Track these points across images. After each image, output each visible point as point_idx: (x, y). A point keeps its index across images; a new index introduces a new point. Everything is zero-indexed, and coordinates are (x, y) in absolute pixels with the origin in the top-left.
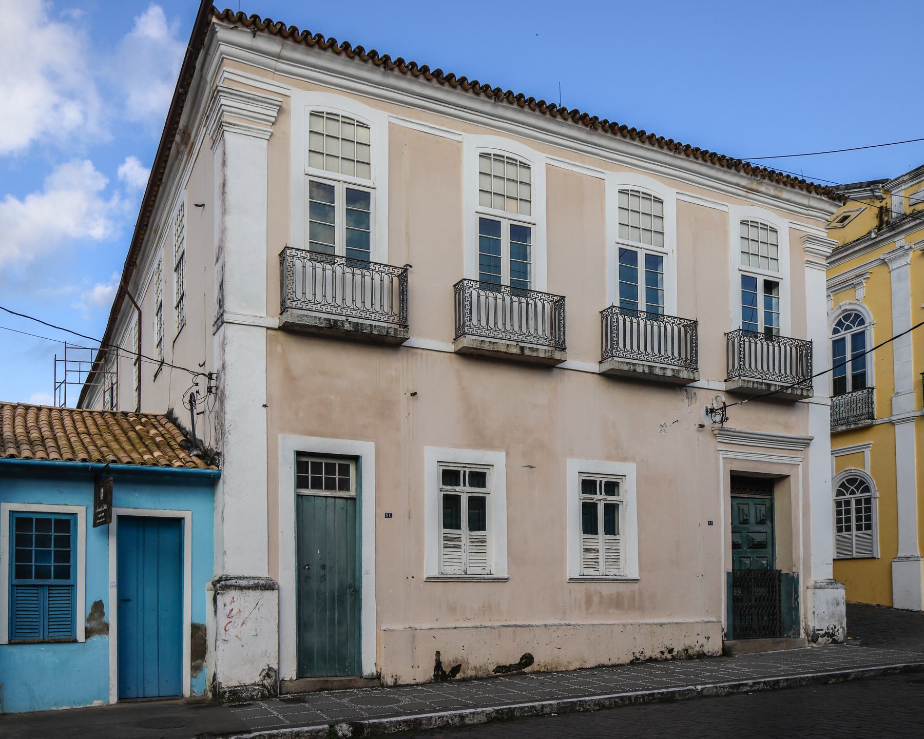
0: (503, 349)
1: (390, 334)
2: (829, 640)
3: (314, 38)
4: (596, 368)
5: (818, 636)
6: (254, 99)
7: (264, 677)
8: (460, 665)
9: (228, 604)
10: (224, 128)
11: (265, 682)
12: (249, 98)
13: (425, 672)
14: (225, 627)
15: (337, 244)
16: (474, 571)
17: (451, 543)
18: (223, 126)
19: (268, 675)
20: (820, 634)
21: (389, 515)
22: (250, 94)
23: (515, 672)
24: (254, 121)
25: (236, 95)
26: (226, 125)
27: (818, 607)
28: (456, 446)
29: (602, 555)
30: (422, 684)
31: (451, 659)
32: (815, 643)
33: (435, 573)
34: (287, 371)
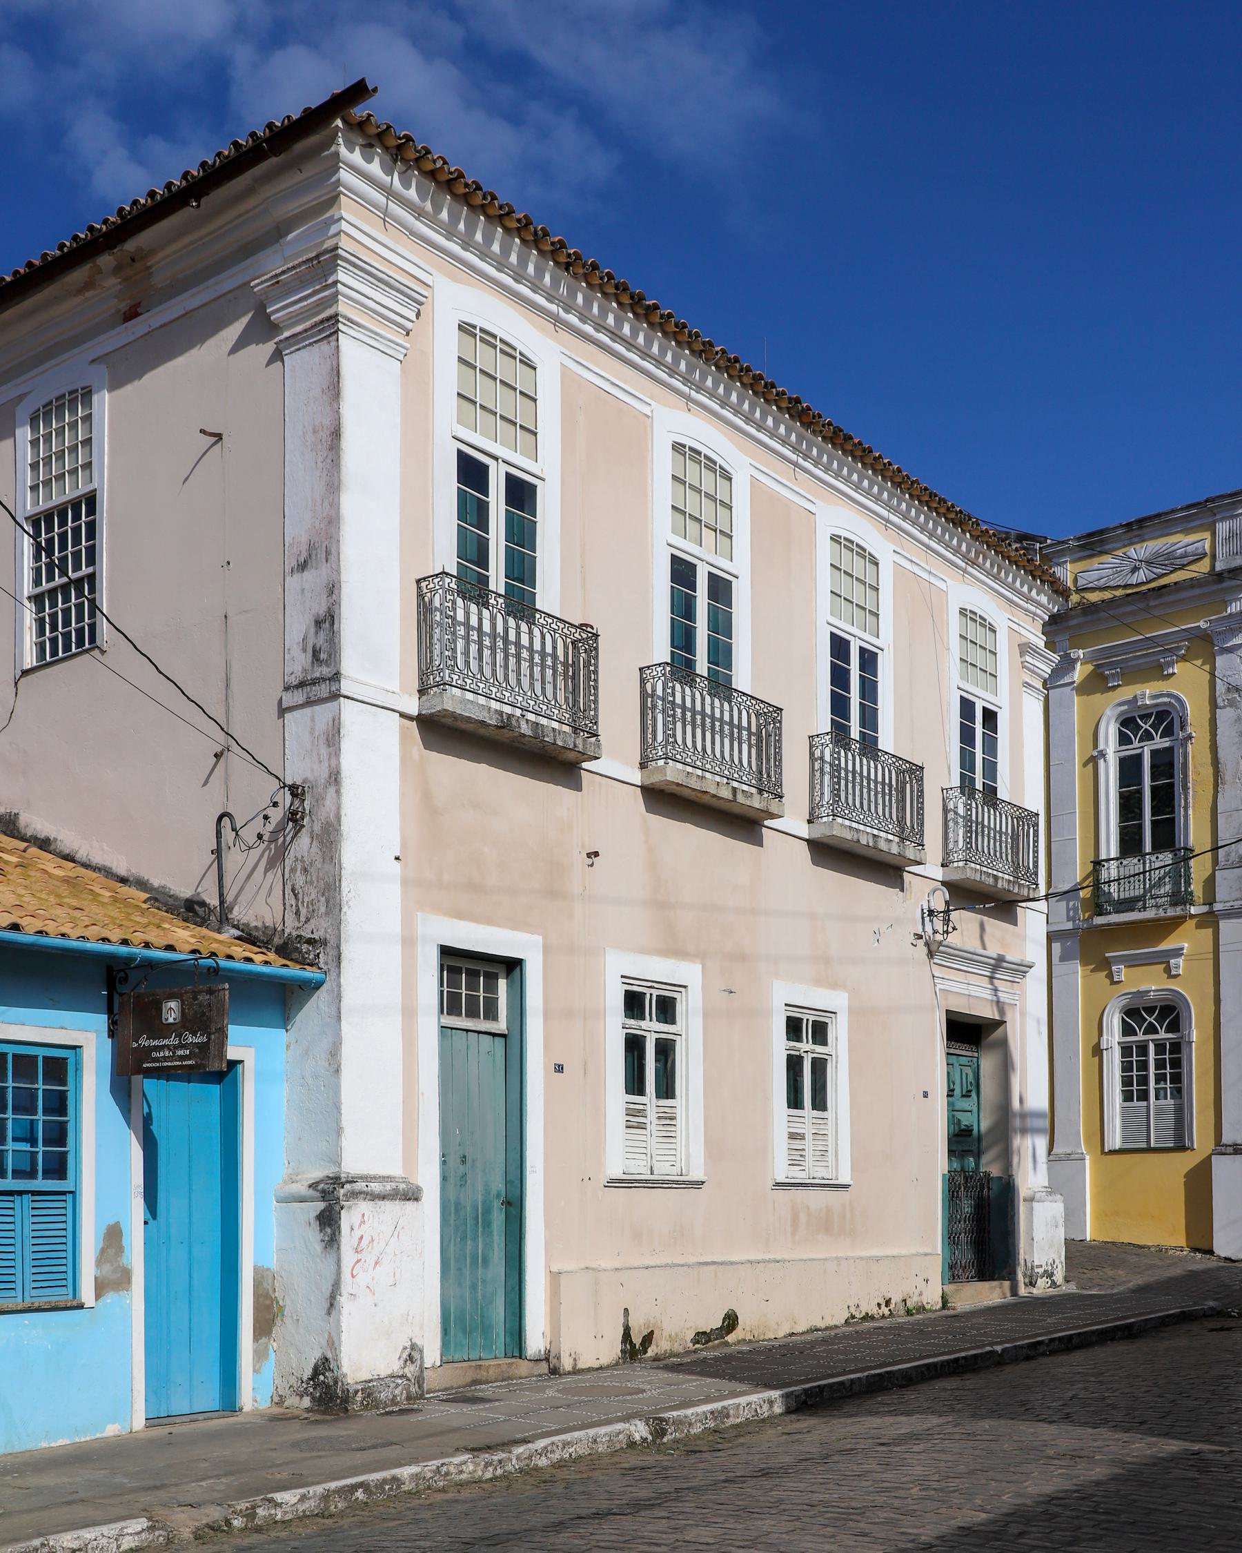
0: (712, 790)
1: (578, 747)
3: (501, 207)
4: (804, 830)
6: (387, 284)
7: (406, 1361)
8: (652, 1332)
9: (356, 1228)
10: (341, 326)
11: (406, 1370)
12: (380, 280)
13: (608, 1350)
14: (352, 1270)
15: (492, 573)
16: (664, 1170)
17: (635, 1122)
18: (338, 321)
19: (411, 1358)
21: (559, 1069)
22: (384, 273)
23: (716, 1342)
24: (380, 322)
25: (362, 270)
26: (344, 321)
28: (644, 951)
29: (808, 1143)
30: (608, 1367)
31: (642, 1322)
33: (617, 1173)
34: (427, 796)
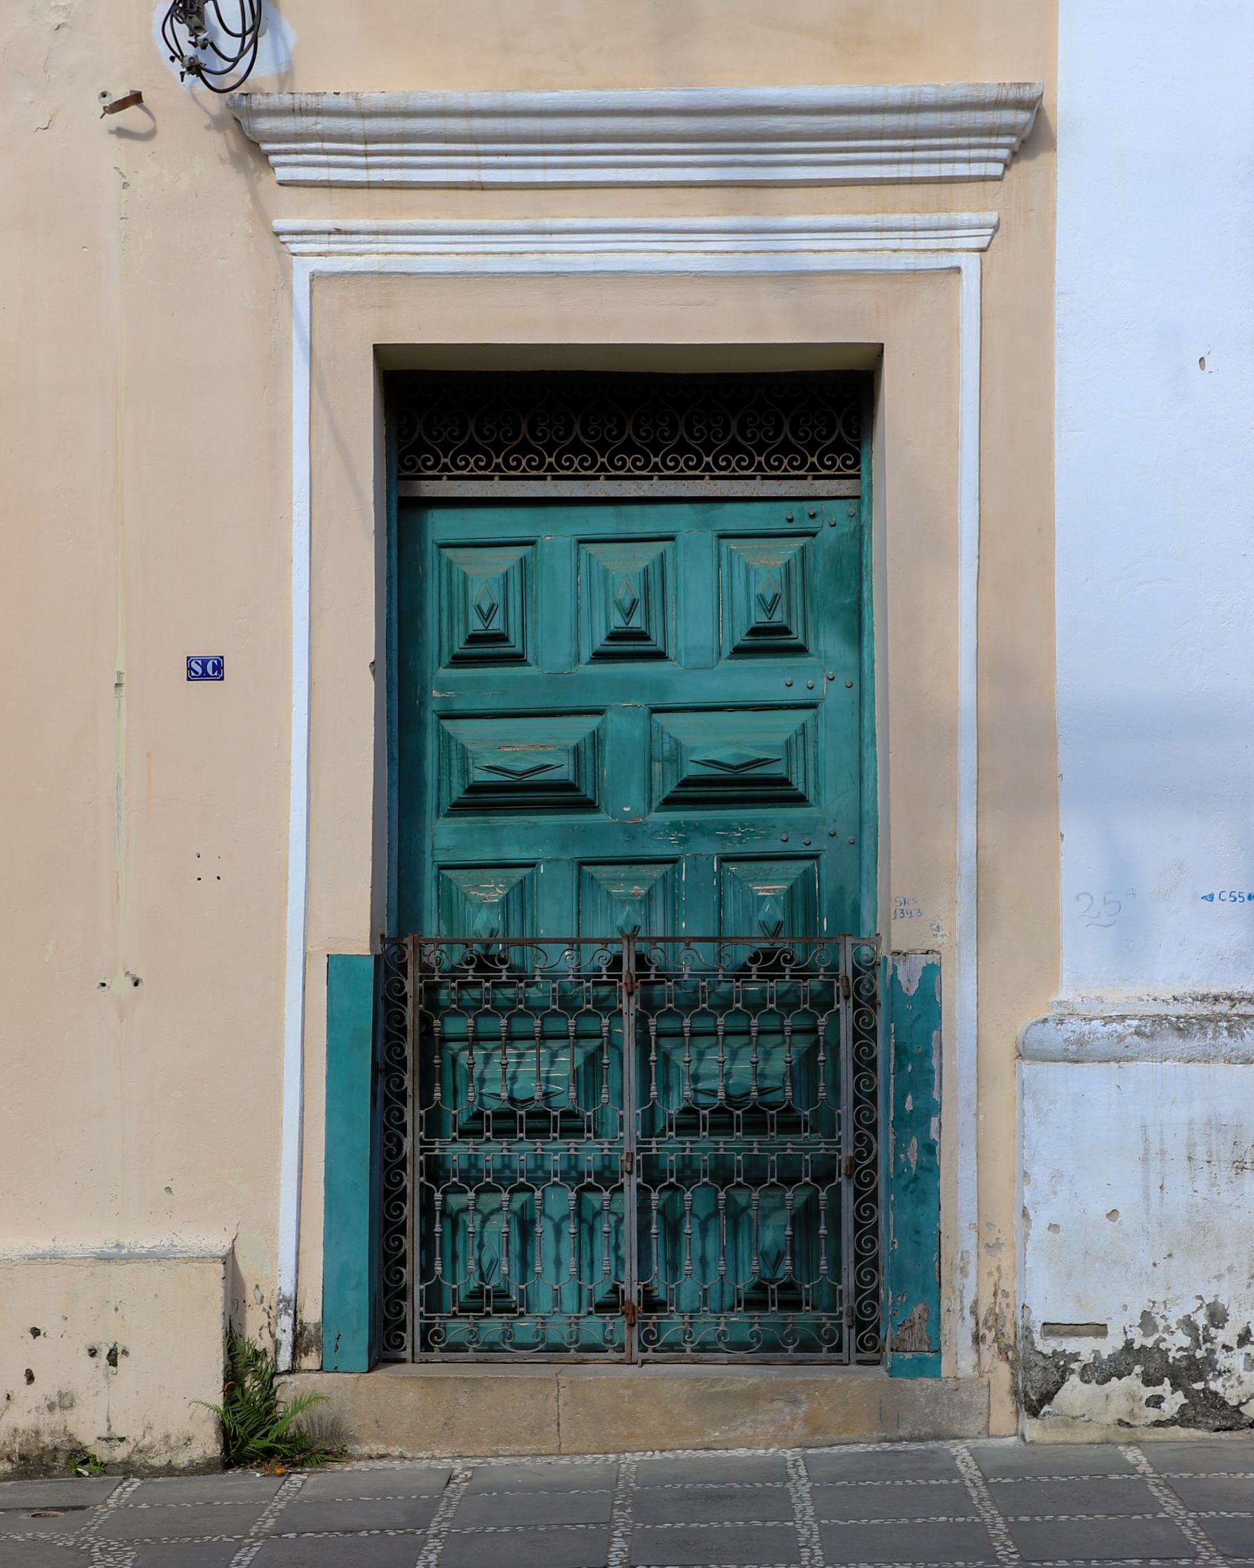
2: (1156, 1401)
5: (1061, 1368)
20: (1075, 1357)
27: (1057, 1176)
32: (1034, 1412)
